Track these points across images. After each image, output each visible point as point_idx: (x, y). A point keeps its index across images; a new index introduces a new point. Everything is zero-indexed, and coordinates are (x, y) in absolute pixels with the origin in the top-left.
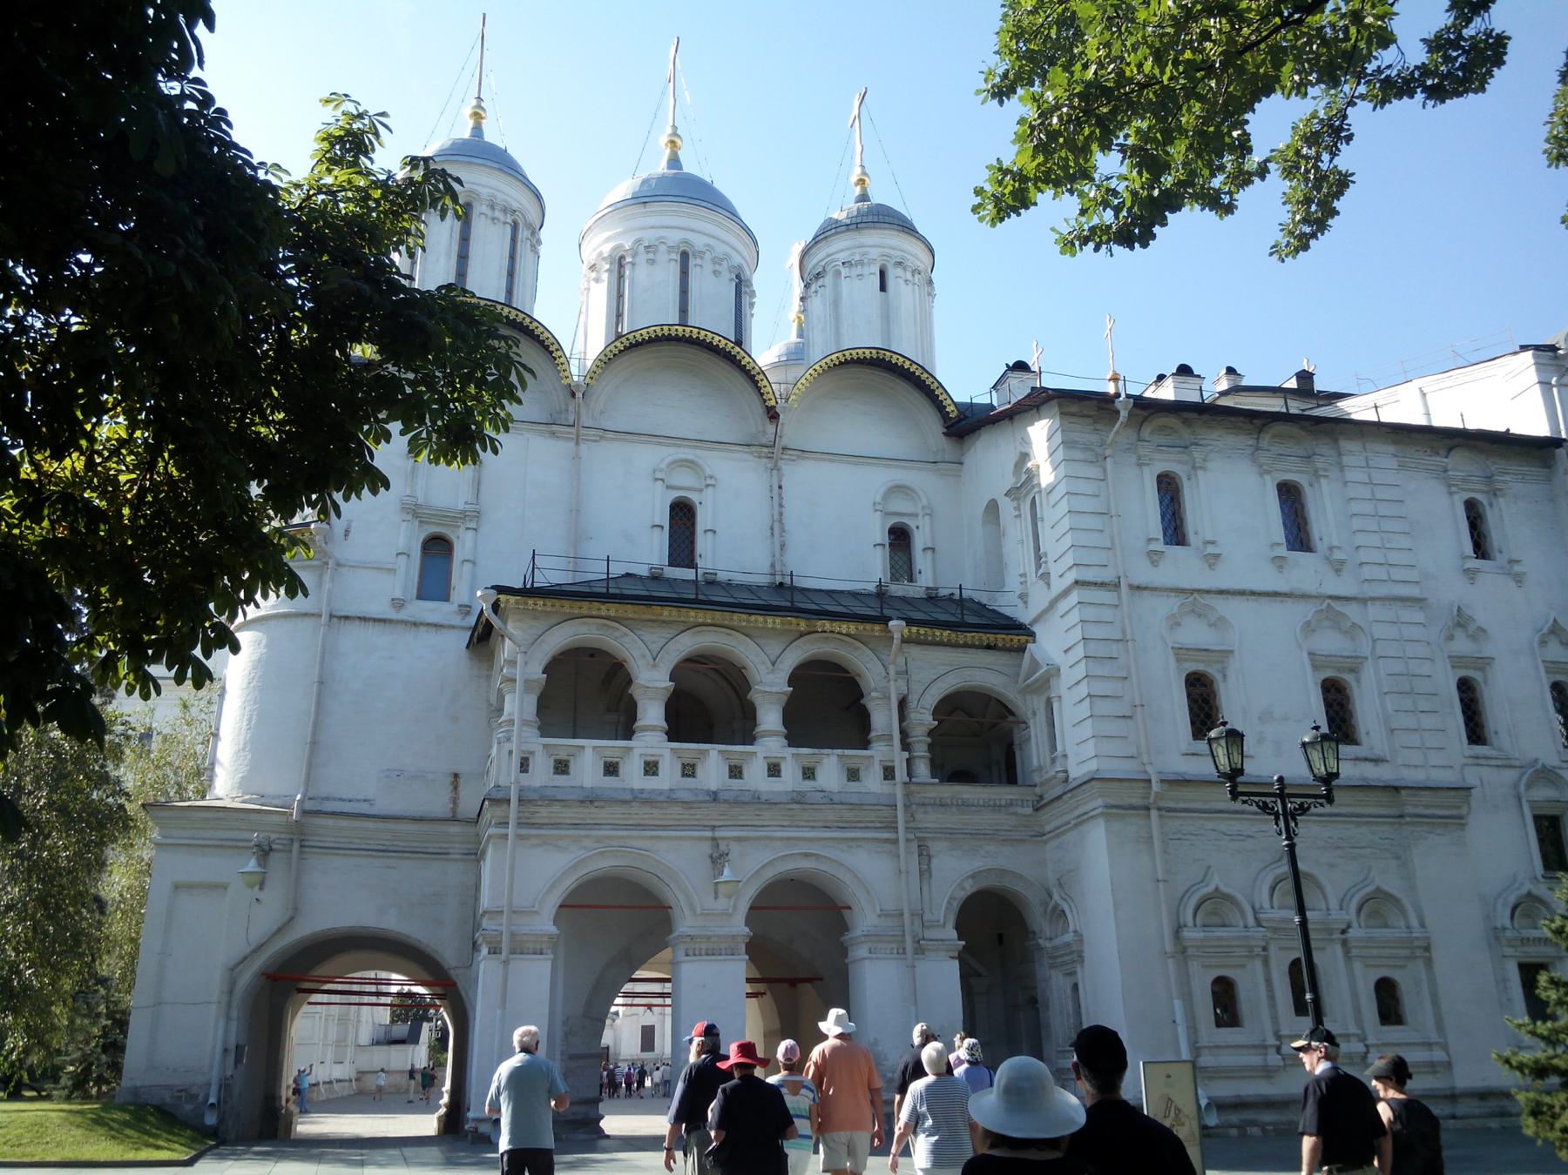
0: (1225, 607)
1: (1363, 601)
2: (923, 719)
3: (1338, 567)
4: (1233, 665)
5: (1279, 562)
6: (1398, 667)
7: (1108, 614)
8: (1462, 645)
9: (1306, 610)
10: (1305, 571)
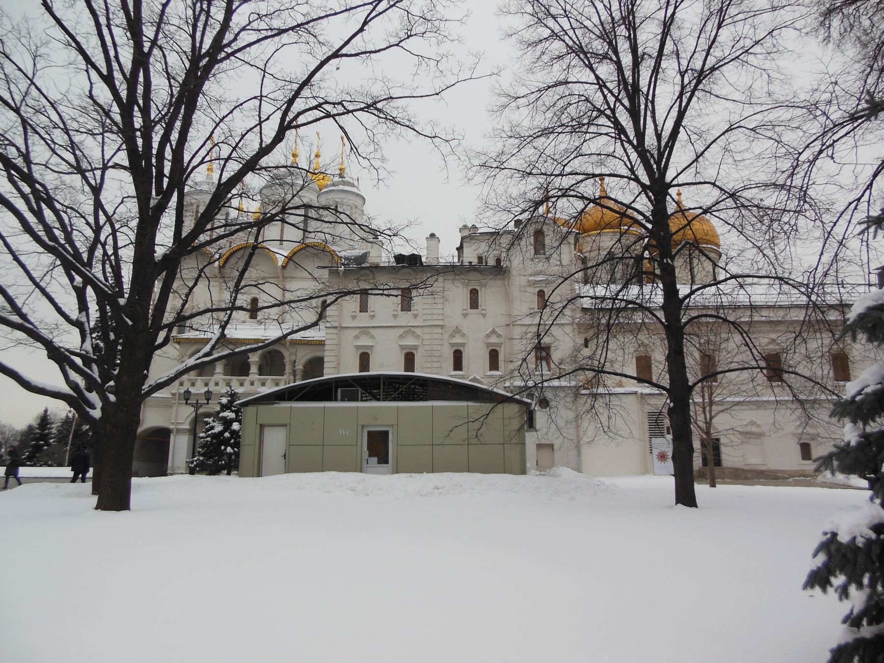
0: (373, 332)
1: (422, 327)
2: (300, 367)
3: (415, 316)
4: (374, 349)
5: (395, 316)
6: (428, 348)
7: (334, 336)
8: (458, 340)
9: (401, 331)
10: (405, 319)
